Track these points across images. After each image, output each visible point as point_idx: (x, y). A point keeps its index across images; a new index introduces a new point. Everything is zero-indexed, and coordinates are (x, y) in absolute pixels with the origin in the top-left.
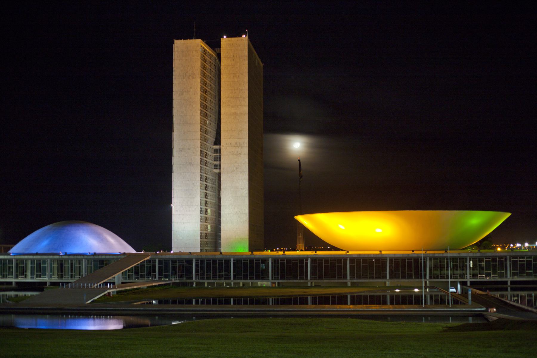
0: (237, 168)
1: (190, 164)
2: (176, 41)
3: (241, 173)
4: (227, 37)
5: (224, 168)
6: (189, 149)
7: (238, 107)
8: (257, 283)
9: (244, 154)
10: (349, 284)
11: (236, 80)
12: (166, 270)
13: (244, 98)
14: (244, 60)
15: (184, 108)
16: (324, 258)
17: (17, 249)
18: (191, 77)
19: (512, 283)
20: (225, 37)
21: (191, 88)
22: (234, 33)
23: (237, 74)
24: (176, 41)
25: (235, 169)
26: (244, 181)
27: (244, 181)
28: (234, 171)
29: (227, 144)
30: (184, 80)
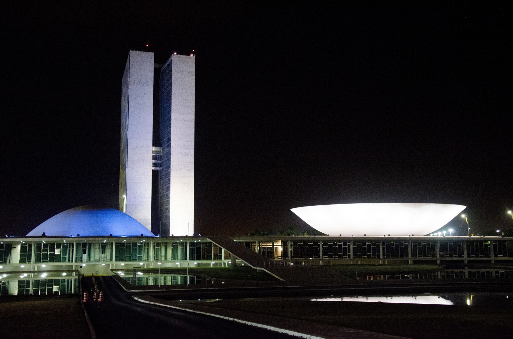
0: (184, 167)
1: (143, 160)
2: (131, 51)
3: (188, 170)
4: (177, 54)
6: (142, 147)
8: (209, 264)
9: (191, 155)
10: (438, 262)
12: (198, 252)
16: (426, 240)
17: (37, 231)
18: (145, 85)
19: (469, 261)
20: (175, 53)
21: (145, 94)
22: (184, 52)
23: (186, 87)
24: (131, 51)
28: (182, 168)
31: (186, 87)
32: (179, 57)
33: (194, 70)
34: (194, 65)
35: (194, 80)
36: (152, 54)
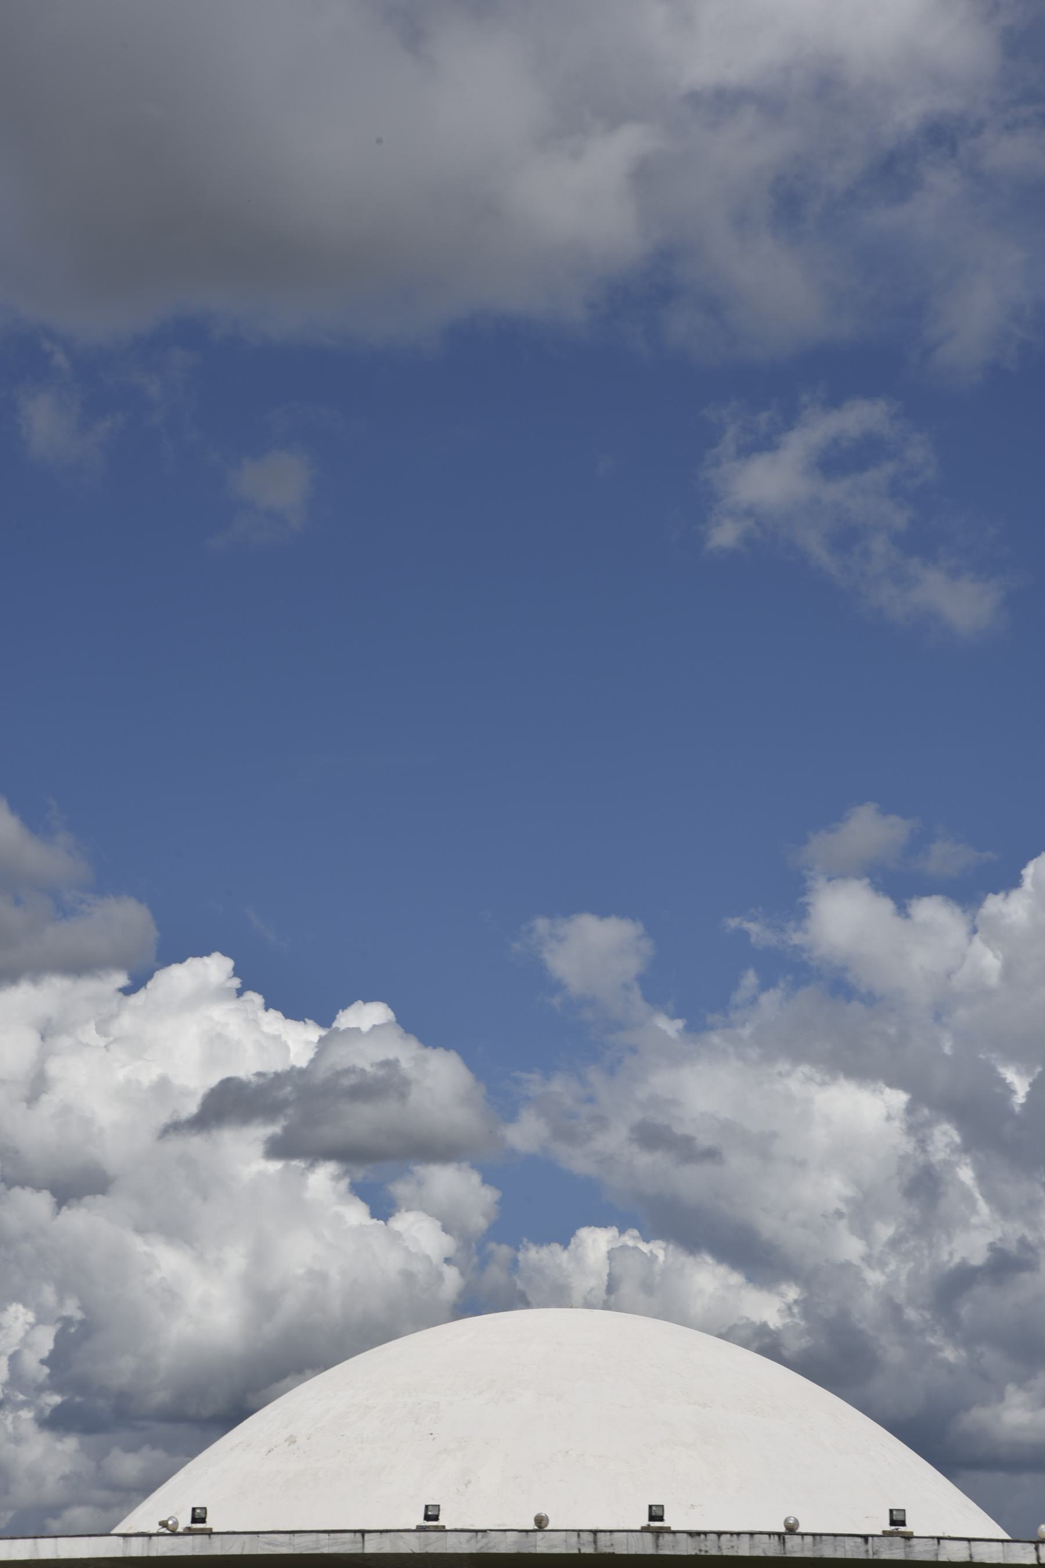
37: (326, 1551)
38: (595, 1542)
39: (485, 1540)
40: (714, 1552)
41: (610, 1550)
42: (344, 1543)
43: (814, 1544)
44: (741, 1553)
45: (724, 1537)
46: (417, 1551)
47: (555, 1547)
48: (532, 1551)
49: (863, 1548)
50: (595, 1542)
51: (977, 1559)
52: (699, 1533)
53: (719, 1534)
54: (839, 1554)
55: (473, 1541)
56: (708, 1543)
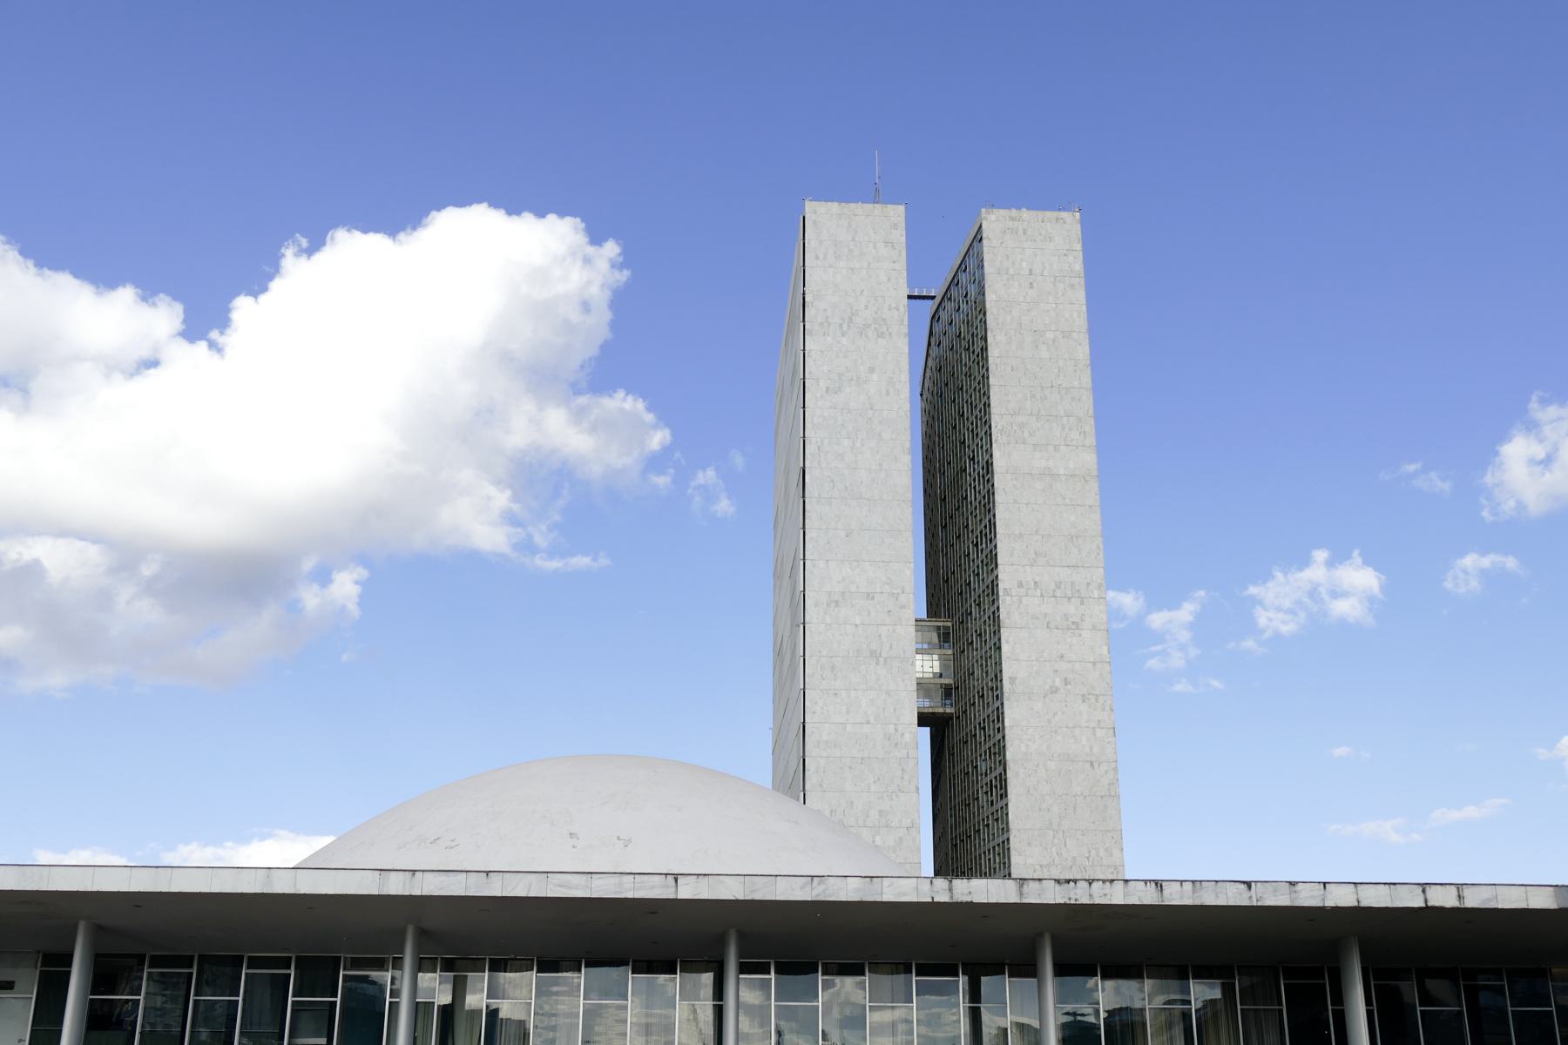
0: (1066, 682)
1: (875, 655)
2: (809, 207)
5: (1013, 680)
6: (869, 596)
7: (1056, 448)
9: (1094, 628)
11: (1044, 352)
13: (1080, 419)
14: (1072, 286)
15: (846, 442)
21: (872, 370)
23: (1050, 335)
25: (1058, 682)
26: (1099, 733)
27: (1099, 733)
28: (1054, 690)
29: (1020, 585)
30: (844, 340)
31: (1050, 335)
32: (1013, 219)
33: (1078, 267)
34: (1079, 247)
35: (1084, 308)
36: (897, 212)
37: (630, 895)
38: (950, 890)
39: (822, 887)
40: (1085, 900)
41: (968, 899)
42: (653, 887)
43: (1194, 891)
44: (1115, 902)
45: (1095, 885)
46: (741, 897)
47: (905, 894)
48: (878, 899)
49: (1246, 894)
50: (950, 890)
51: (1364, 904)
52: (1068, 881)
53: (1090, 882)
54: (1221, 901)
55: (808, 888)
56: (1079, 891)
